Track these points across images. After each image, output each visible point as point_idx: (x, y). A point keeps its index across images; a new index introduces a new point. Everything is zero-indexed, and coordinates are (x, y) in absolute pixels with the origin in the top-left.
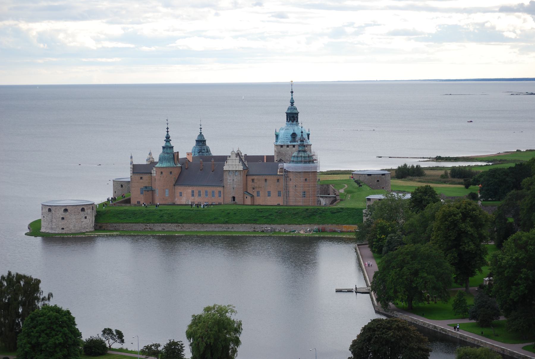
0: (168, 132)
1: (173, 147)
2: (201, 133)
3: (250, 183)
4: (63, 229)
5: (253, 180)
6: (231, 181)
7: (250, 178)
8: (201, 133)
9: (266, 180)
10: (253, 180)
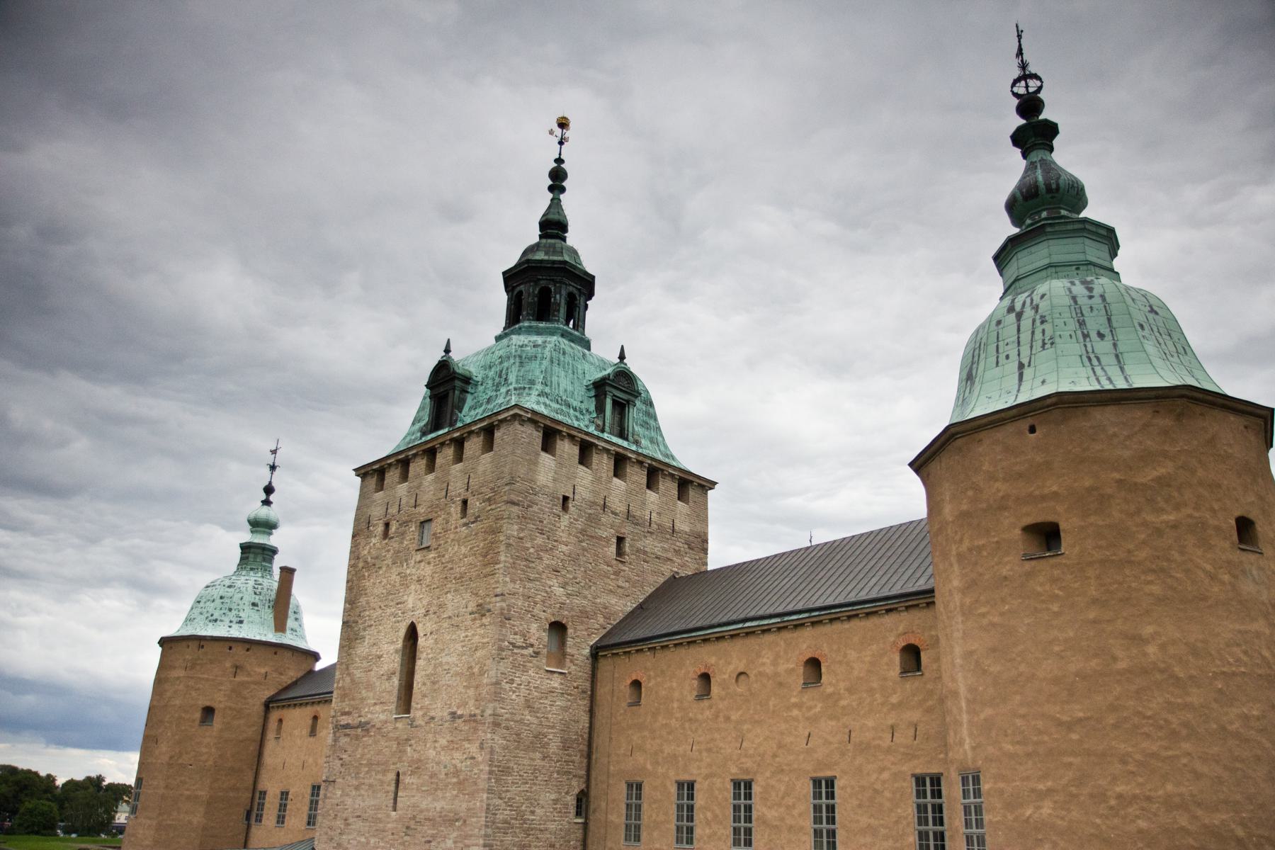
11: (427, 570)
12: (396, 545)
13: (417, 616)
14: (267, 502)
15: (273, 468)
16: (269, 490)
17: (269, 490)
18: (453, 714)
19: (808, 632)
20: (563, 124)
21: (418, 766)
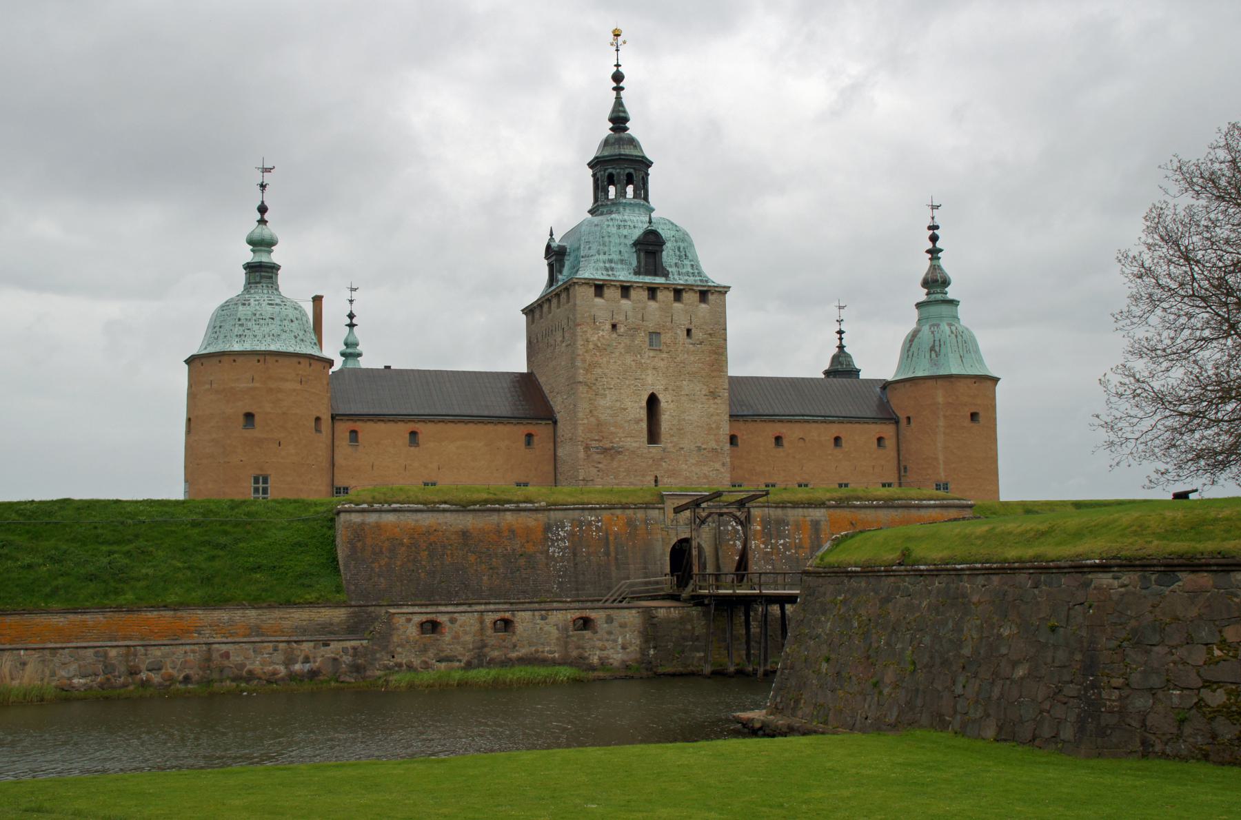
0: (351, 326)
2: (841, 347)
8: (841, 347)
11: (661, 364)
12: (628, 342)
13: (658, 389)
14: (262, 222)
15: (263, 186)
16: (263, 209)
17: (263, 209)
18: (699, 448)
19: (836, 426)
21: (673, 473)
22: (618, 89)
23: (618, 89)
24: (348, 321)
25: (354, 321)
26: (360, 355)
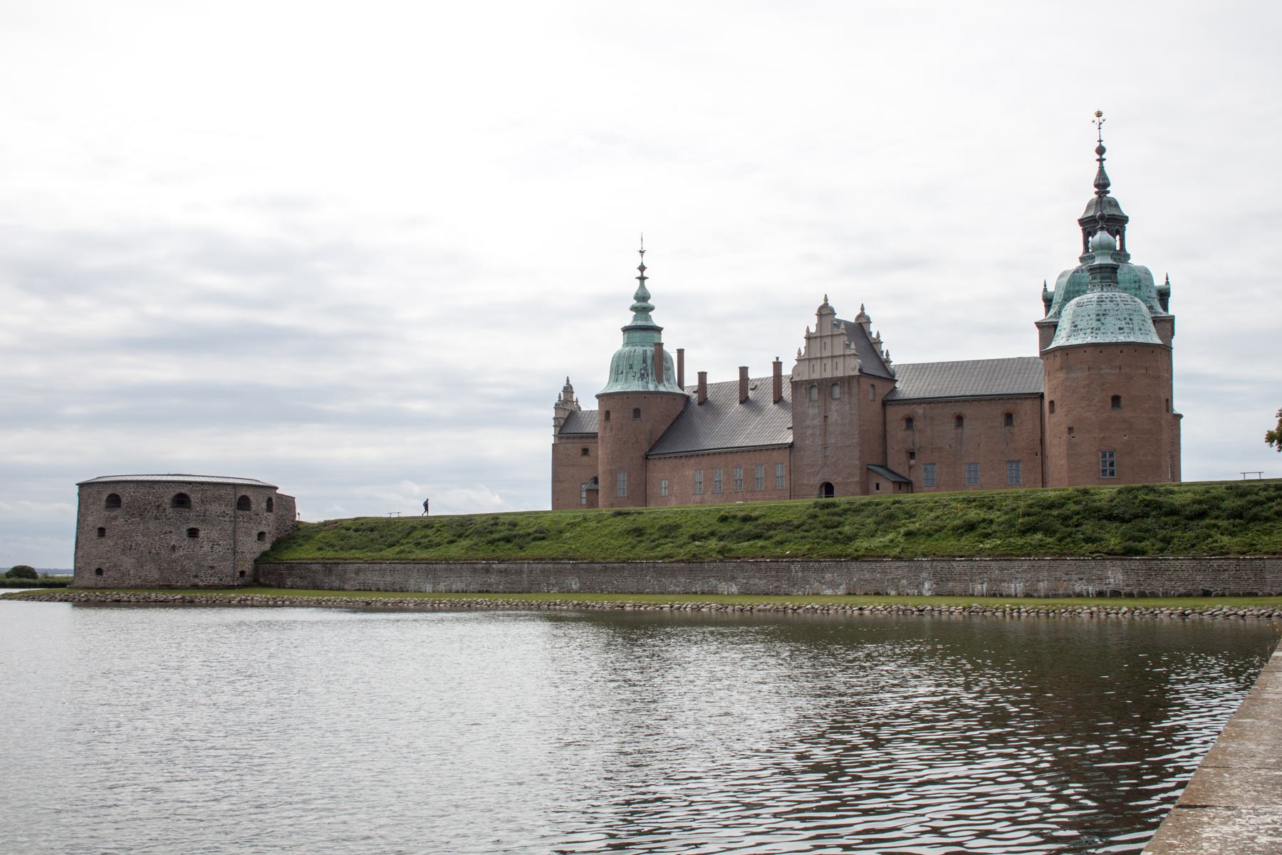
0: (642, 279)
1: (659, 330)
3: (897, 433)
4: (99, 572)
5: (909, 421)
6: (818, 421)
7: (895, 414)
9: (960, 419)
10: (909, 421)
20: (1099, 114)
22: (1101, 160)
23: (1101, 160)
24: (639, 274)
25: (645, 274)
26: (652, 309)
